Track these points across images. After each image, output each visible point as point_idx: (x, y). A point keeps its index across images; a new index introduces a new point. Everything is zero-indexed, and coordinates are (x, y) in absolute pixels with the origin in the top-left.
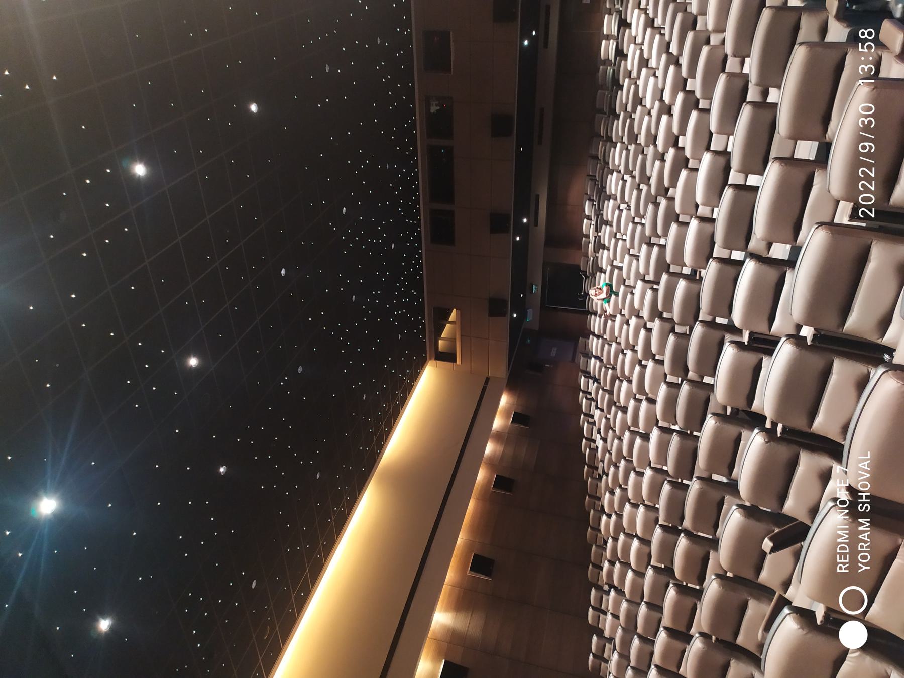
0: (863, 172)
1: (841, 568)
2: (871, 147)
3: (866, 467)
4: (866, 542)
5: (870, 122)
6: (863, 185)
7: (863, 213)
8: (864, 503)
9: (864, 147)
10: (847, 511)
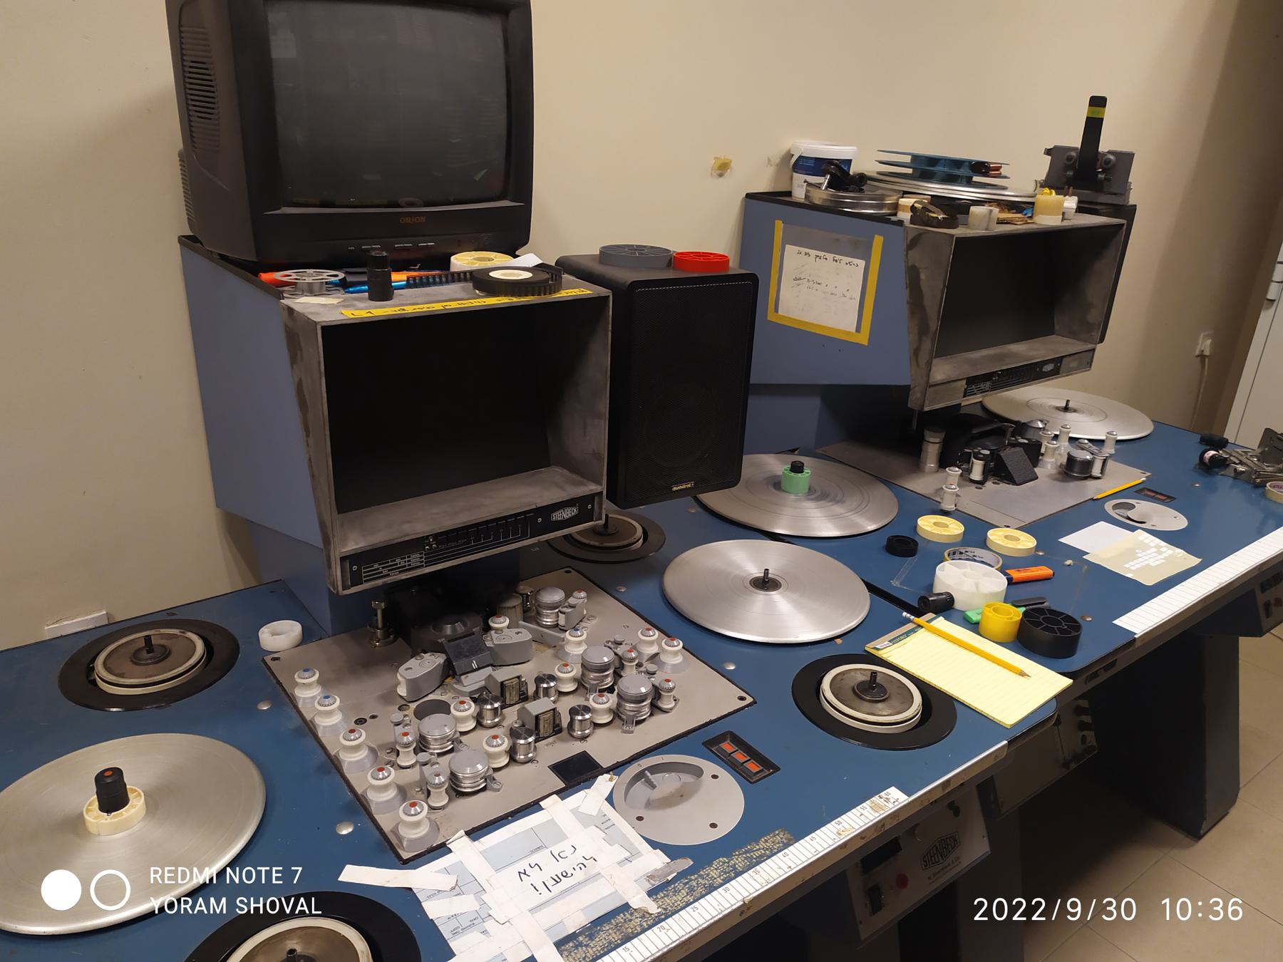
0: (1039, 904)
1: (156, 872)
2: (1074, 915)
3: (299, 908)
4: (193, 908)
5: (1110, 914)
6: (1020, 904)
7: (981, 904)
8: (248, 905)
9: (1074, 905)
10: (237, 881)
